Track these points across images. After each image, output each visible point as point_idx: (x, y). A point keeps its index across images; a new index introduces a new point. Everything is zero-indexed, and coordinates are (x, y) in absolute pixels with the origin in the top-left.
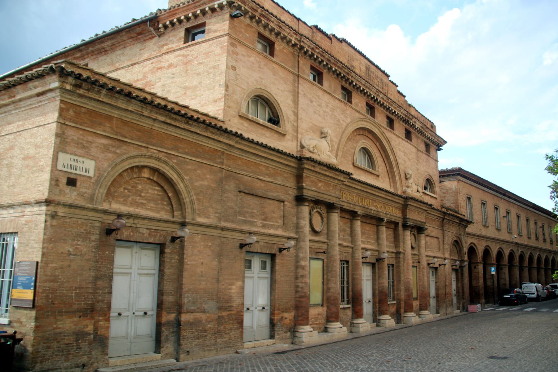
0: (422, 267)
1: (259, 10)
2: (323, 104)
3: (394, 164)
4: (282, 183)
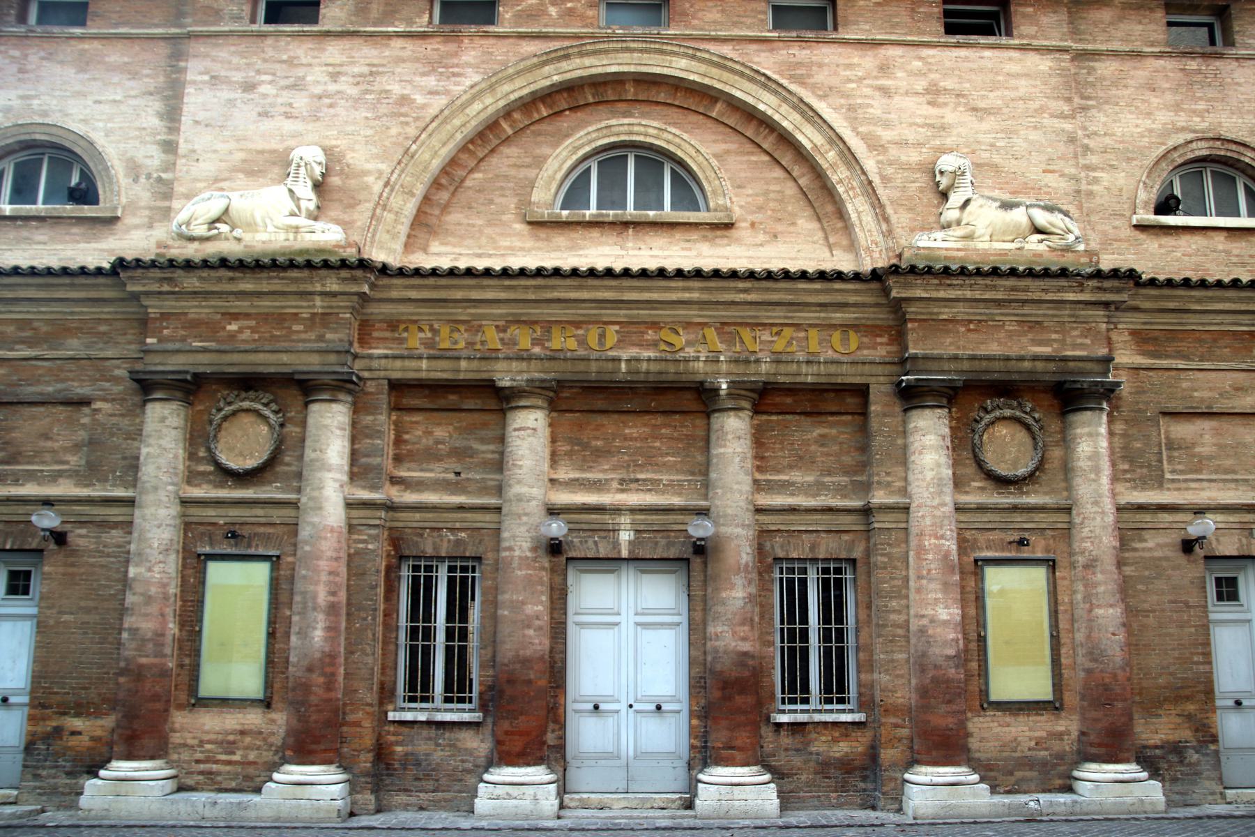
0: (1081, 560)
2: (316, 77)
3: (828, 158)
4: (82, 354)
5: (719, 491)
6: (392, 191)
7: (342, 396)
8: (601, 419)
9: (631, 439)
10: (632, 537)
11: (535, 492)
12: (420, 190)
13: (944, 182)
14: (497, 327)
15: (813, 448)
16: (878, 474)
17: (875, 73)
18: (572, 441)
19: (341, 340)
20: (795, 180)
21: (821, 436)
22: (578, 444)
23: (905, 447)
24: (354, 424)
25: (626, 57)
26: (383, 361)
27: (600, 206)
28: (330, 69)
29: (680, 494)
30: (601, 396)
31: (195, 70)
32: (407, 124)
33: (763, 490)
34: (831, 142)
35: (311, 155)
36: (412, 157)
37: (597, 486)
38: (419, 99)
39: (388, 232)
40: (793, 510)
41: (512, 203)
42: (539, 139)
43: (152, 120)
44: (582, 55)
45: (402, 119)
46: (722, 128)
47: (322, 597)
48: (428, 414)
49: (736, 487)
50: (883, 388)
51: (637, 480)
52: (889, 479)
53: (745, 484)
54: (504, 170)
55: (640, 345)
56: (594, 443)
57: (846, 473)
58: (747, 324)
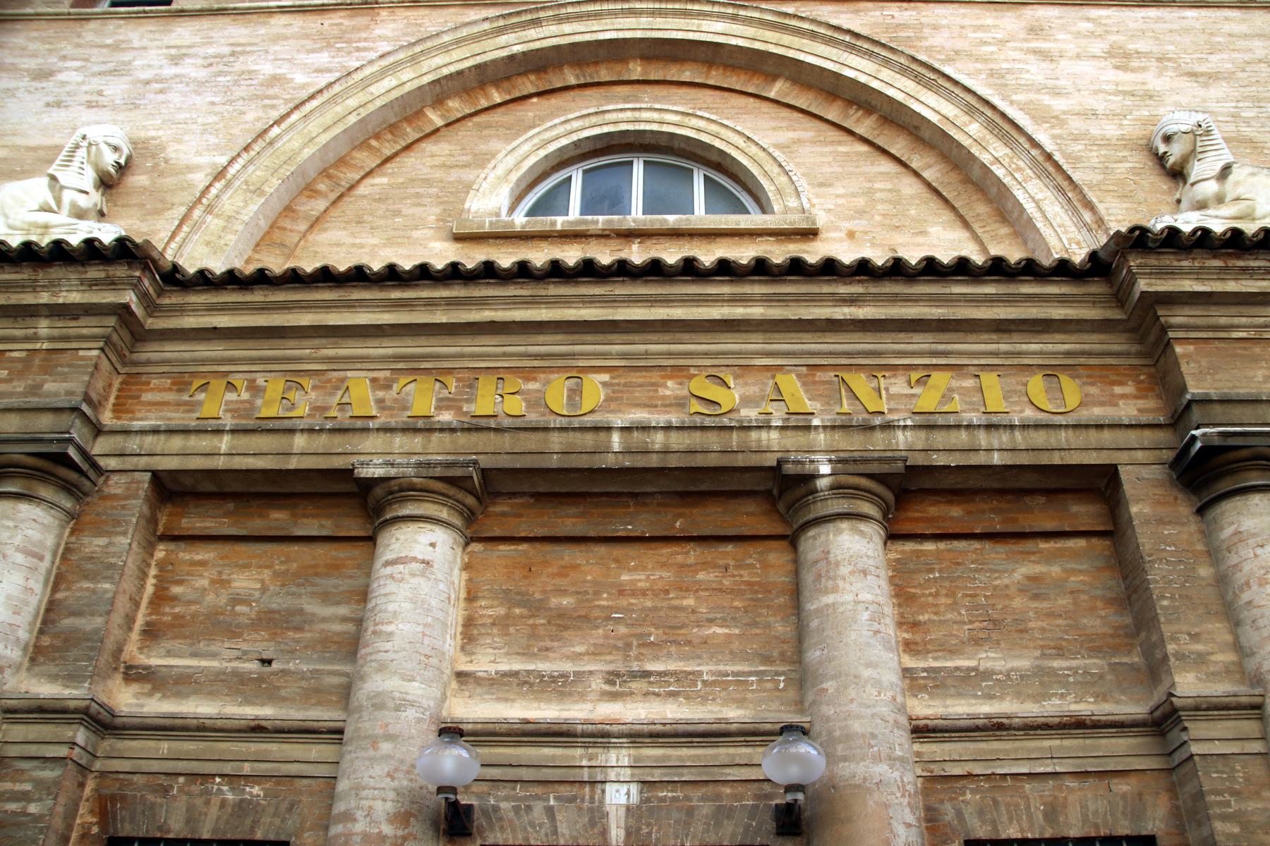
3: (970, 132)
5: (830, 685)
6: (227, 186)
7: (45, 492)
8: (569, 554)
9: (634, 593)
10: (635, 799)
11: (415, 689)
13: (1175, 152)
14: (374, 380)
15: (1017, 603)
16: (1174, 639)
17: (1023, 35)
18: (508, 597)
19: (70, 393)
20: (916, 174)
21: (1029, 578)
22: (519, 605)
23: (1222, 581)
25: (630, 22)
26: (149, 439)
27: (585, 210)
28: (173, 51)
29: (741, 702)
30: (573, 510)
33: (924, 688)
34: (970, 111)
36: (271, 143)
37: (558, 686)
39: (208, 243)
40: (996, 728)
41: (432, 214)
42: (486, 132)
44: (559, 20)
45: (267, 102)
46: (785, 113)
48: (227, 548)
49: (866, 673)
50: (1145, 472)
51: (646, 674)
52: (1199, 647)
53: (891, 676)
54: (425, 171)
55: (650, 406)
56: (554, 601)
57: (1095, 651)
58: (860, 367)
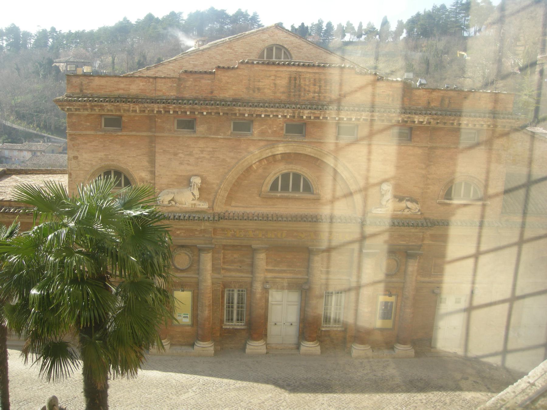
1: (88, 104)
12: (229, 189)
13: (383, 193)
24: (213, 256)
28: (200, 149)
31: (158, 148)
32: (224, 168)
35: (197, 181)
38: (228, 160)
43: (145, 163)
47: (207, 303)
